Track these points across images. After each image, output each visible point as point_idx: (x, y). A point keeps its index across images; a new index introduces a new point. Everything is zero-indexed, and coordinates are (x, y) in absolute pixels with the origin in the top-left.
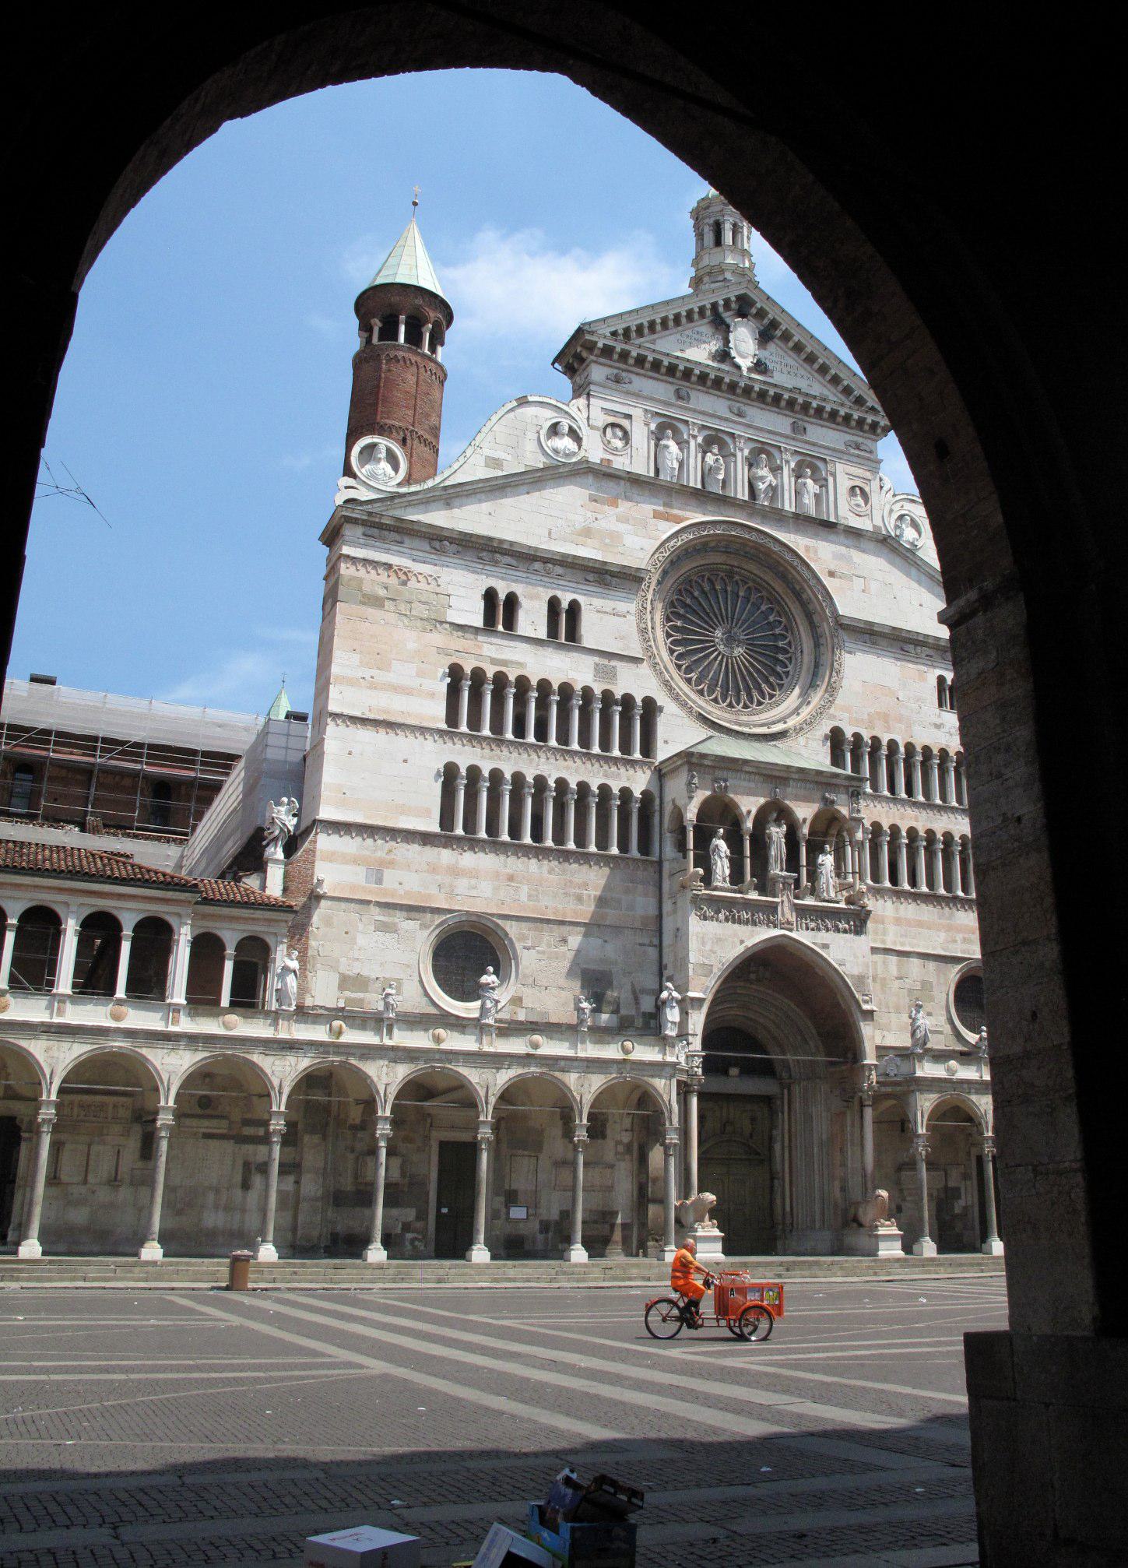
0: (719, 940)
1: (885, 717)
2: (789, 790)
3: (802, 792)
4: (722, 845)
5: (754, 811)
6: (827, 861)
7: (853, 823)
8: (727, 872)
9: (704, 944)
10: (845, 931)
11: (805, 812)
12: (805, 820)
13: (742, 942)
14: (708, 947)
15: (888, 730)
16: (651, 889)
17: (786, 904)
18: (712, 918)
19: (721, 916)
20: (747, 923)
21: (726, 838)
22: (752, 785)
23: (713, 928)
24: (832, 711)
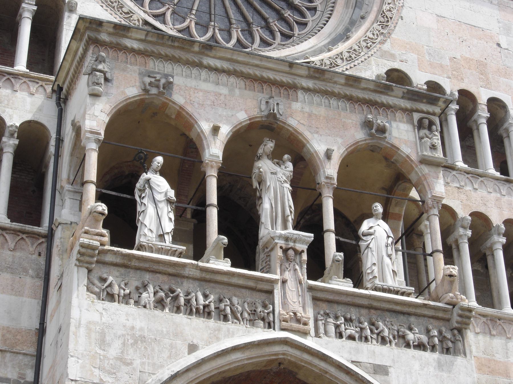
0: (139, 340)
1: (481, 67)
2: (296, 106)
3: (322, 111)
4: (162, 186)
5: (225, 130)
6: (378, 233)
7: (426, 169)
8: (169, 226)
9: (103, 343)
10: (420, 346)
11: (330, 139)
12: (328, 155)
13: (192, 348)
14: (114, 351)
15: (487, 85)
16: (31, 283)
17: (291, 285)
18: (126, 299)
19: (148, 296)
20: (205, 312)
21: (163, 172)
22: (224, 91)
23: (123, 316)
24: (386, 46)
